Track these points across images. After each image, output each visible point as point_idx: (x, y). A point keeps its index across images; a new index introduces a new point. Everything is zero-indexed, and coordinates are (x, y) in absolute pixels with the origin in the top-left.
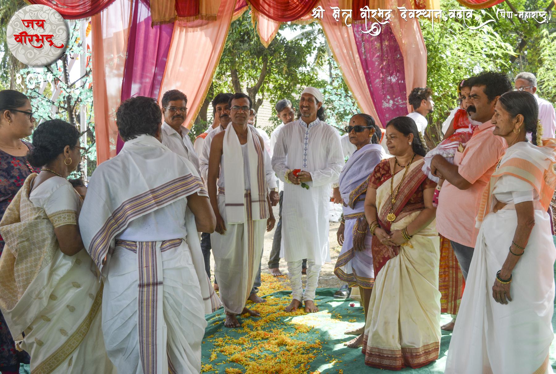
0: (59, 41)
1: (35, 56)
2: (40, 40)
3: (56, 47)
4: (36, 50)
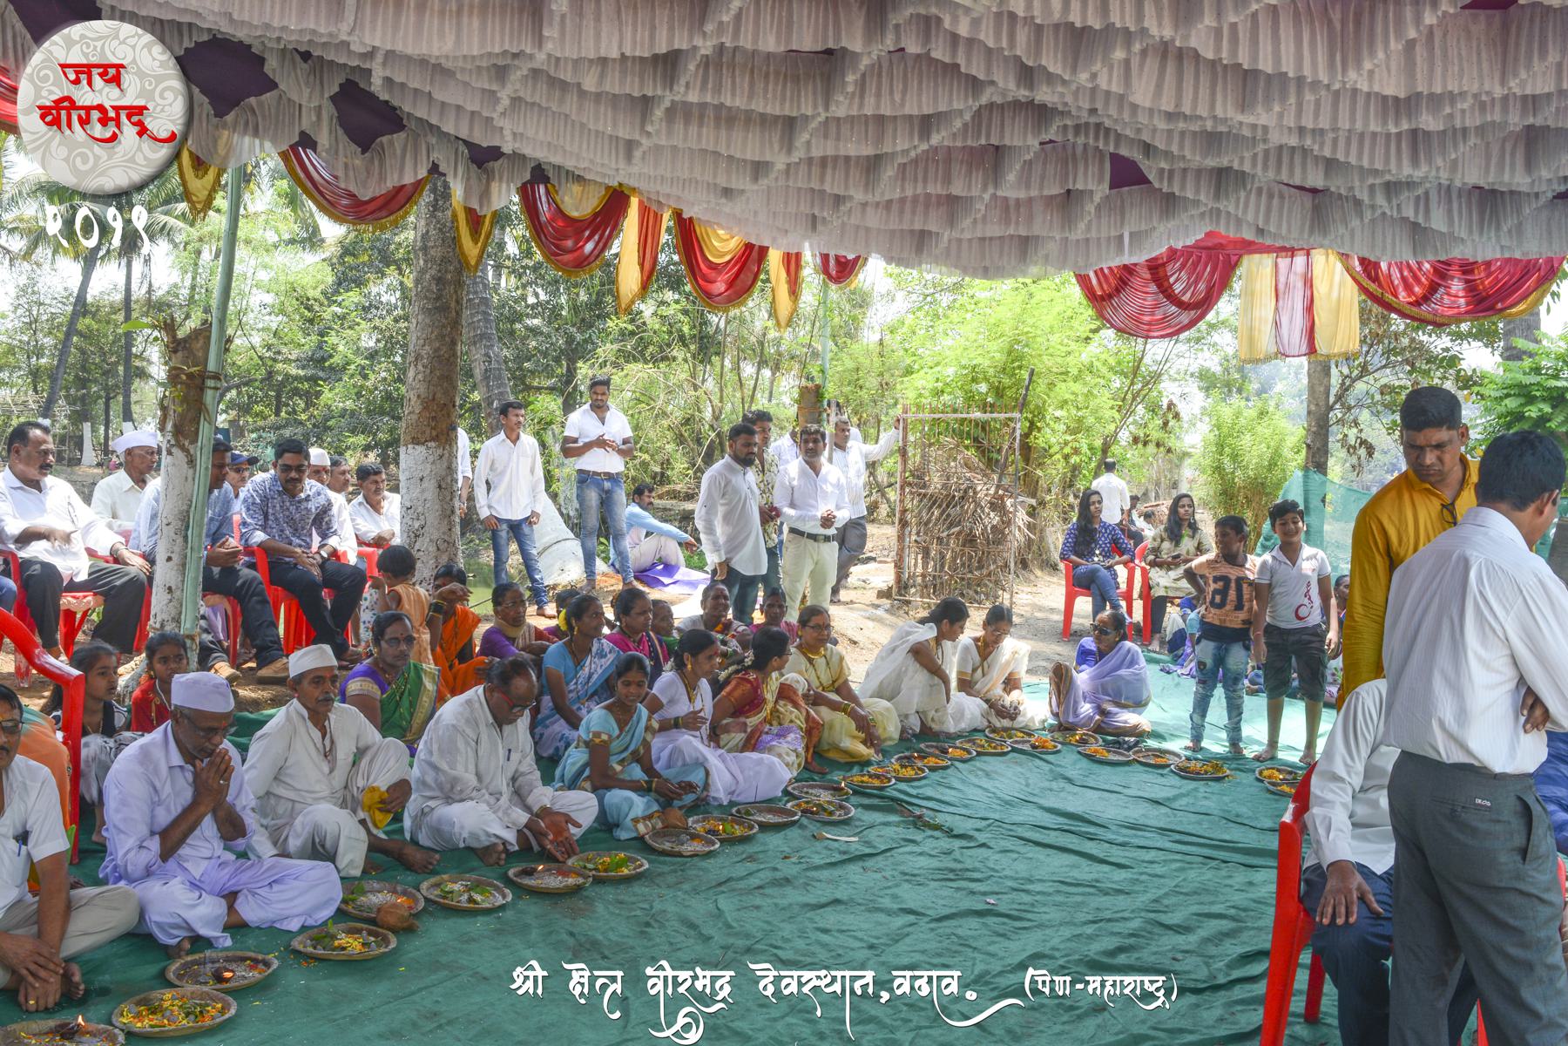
1: (96, 165)
2: (112, 119)
3: (156, 139)
4: (98, 149)
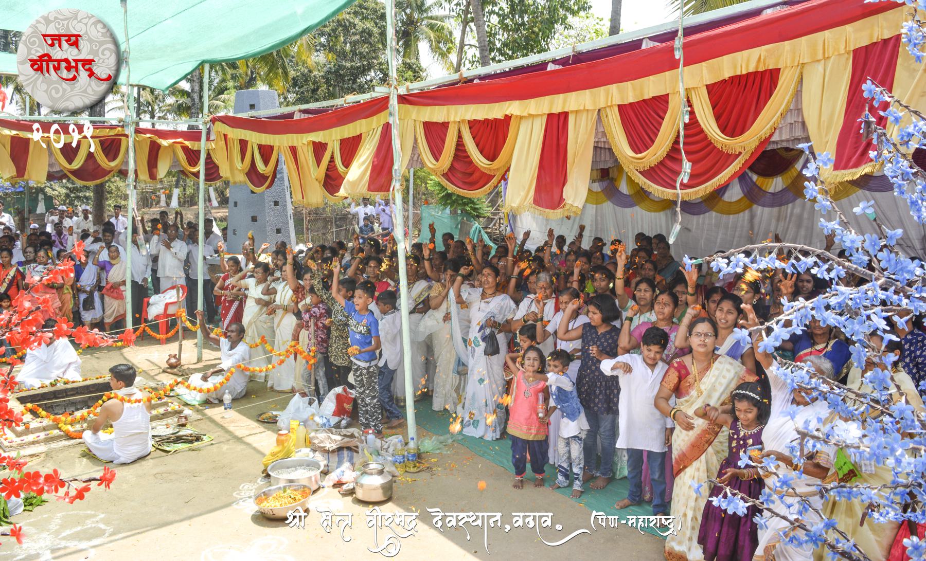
0: (103, 68)
2: (73, 67)
3: (99, 79)
4: (65, 85)
